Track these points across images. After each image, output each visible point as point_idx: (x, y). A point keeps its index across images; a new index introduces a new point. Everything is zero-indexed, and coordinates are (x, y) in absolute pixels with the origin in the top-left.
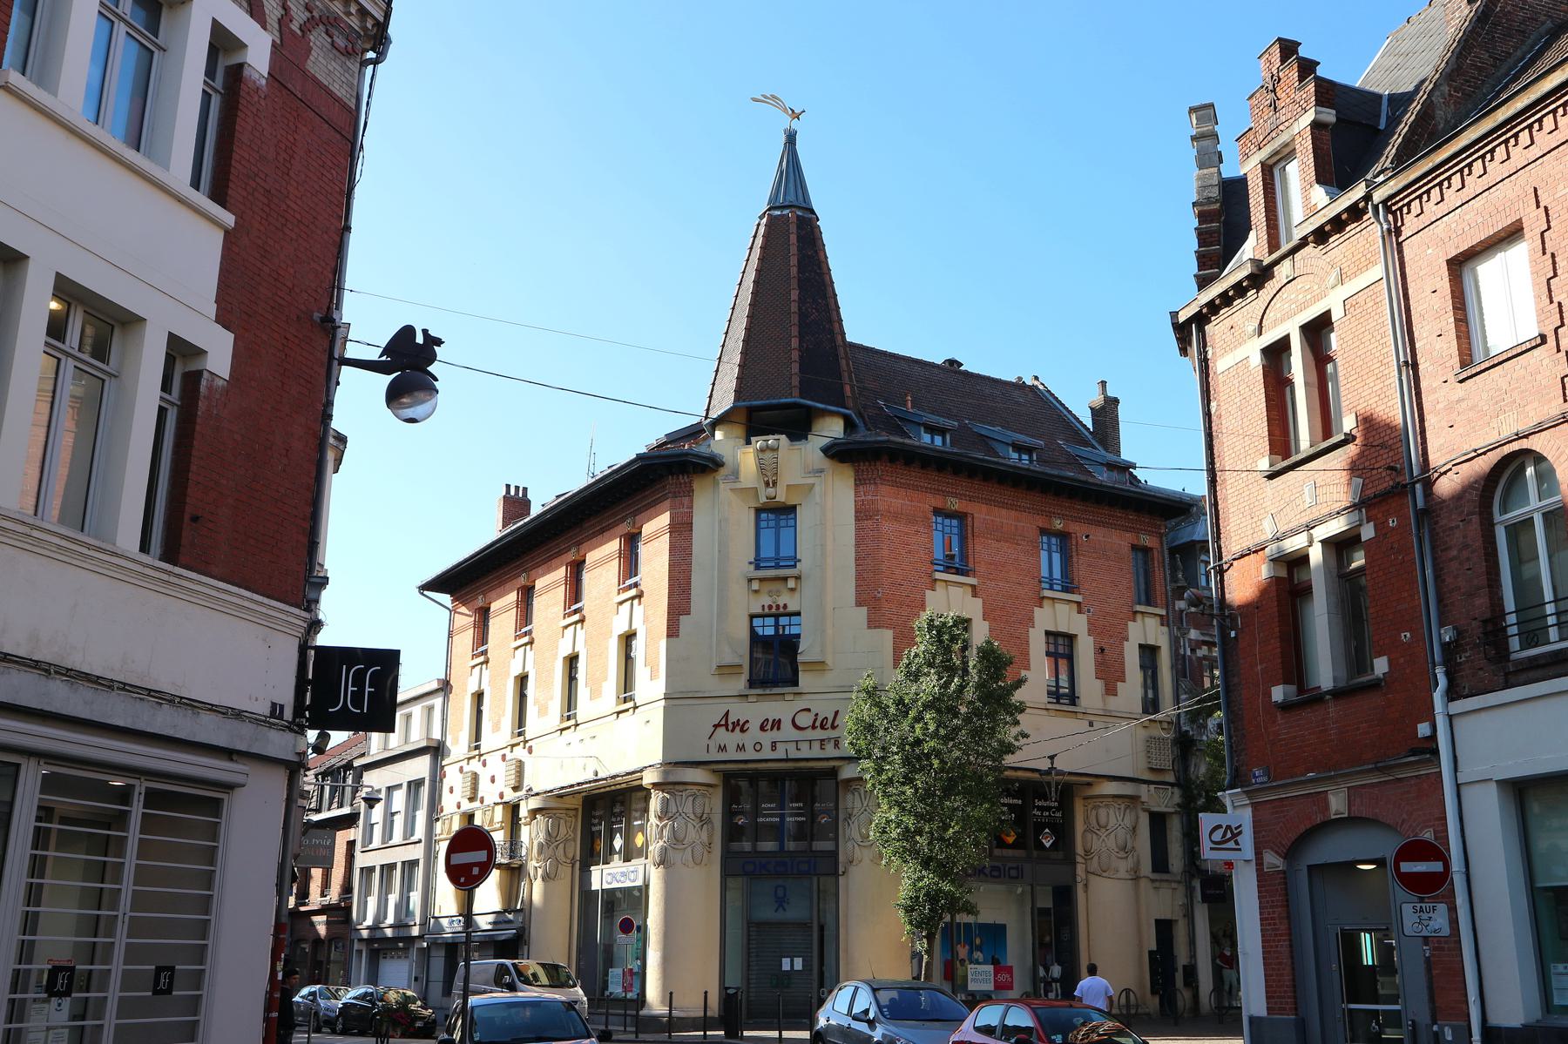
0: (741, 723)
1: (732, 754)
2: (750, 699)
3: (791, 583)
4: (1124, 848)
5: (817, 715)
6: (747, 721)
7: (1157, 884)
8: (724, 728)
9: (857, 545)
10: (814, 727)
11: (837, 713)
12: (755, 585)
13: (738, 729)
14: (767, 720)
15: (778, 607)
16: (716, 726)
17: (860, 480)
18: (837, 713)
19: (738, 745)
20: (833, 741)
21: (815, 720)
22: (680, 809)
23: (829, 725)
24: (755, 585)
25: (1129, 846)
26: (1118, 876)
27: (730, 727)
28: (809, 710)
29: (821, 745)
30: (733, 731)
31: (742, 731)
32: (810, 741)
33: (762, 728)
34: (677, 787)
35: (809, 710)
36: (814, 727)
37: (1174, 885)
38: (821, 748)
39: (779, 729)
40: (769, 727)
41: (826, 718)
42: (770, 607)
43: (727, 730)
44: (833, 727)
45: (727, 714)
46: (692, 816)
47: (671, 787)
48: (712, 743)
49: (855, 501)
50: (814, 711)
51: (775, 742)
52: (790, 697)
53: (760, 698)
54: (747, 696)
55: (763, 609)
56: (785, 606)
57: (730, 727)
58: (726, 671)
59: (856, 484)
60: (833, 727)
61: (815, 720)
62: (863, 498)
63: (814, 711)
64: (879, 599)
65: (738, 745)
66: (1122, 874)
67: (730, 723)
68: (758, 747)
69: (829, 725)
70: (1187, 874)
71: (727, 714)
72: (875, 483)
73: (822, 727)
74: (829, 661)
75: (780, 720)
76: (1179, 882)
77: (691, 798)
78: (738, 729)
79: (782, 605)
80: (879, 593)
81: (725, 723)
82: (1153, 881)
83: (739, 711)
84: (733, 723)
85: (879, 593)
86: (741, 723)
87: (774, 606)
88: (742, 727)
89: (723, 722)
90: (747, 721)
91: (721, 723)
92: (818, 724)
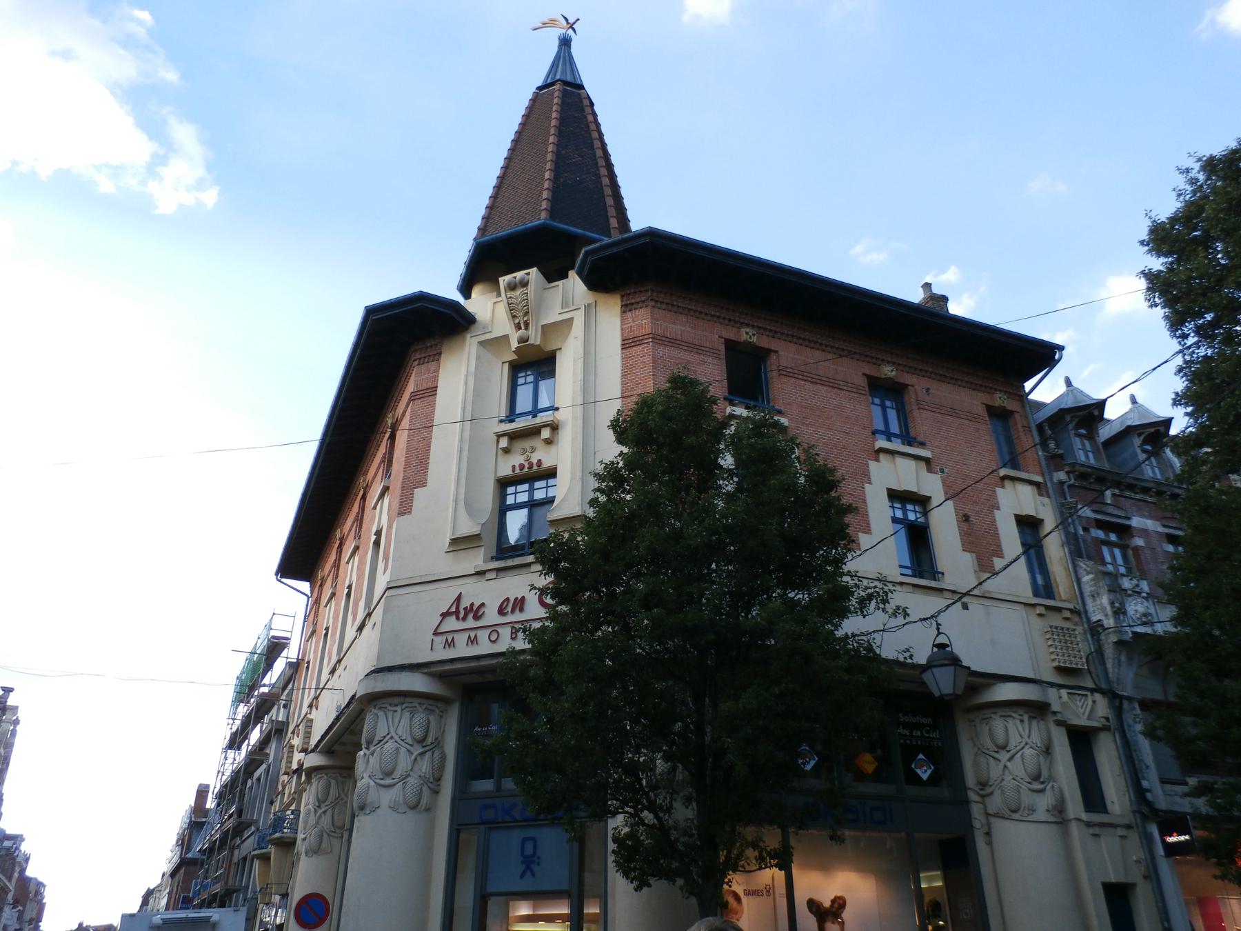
0: (475, 609)
1: (463, 649)
3: (546, 433)
4: (1037, 778)
7: (1097, 830)
8: (453, 618)
12: (504, 443)
13: (471, 616)
14: (508, 599)
16: (445, 615)
22: (392, 730)
25: (1045, 773)
26: (1035, 817)
27: (462, 615)
30: (464, 619)
31: (476, 618)
33: (501, 611)
37: (1120, 832)
39: (521, 610)
40: (509, 609)
42: (522, 467)
43: (458, 618)
55: (514, 471)
57: (462, 615)
66: (1041, 815)
68: (494, 637)
70: (1137, 815)
76: (1129, 827)
78: (471, 616)
79: (535, 462)
81: (456, 610)
82: (1089, 824)
83: (475, 592)
84: (465, 609)
86: (475, 609)
88: (476, 612)
89: (453, 609)
90: (483, 605)
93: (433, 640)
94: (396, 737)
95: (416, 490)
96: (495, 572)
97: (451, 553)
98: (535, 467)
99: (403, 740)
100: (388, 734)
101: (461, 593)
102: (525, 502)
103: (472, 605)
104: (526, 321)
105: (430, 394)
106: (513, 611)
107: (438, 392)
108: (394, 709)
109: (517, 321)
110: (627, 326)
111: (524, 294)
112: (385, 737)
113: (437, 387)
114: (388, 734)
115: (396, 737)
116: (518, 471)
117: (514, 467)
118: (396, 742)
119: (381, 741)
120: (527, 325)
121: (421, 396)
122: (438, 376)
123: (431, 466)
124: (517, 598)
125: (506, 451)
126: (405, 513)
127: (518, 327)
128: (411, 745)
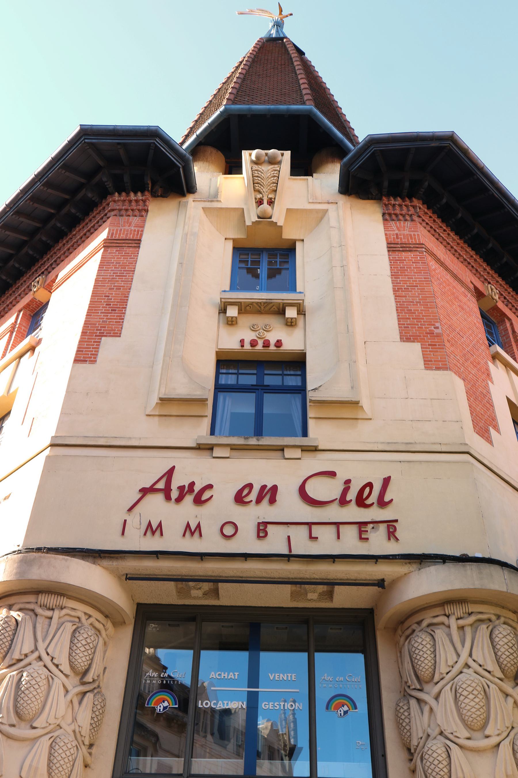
0: (197, 488)
2: (217, 452)
5: (348, 482)
6: (210, 487)
8: (160, 497)
9: (394, 275)
10: (343, 501)
11: (387, 481)
12: (232, 312)
14: (250, 486)
15: (267, 344)
16: (145, 492)
17: (390, 214)
18: (387, 481)
19: (188, 525)
20: (383, 528)
21: (346, 491)
22: (41, 646)
23: (373, 498)
24: (232, 312)
27: (175, 494)
28: (332, 474)
29: (361, 532)
30: (179, 500)
31: (198, 501)
32: (337, 524)
34: (43, 599)
35: (332, 474)
36: (343, 501)
38: (361, 538)
39: (272, 501)
40: (253, 496)
41: (370, 485)
42: (253, 343)
43: (168, 498)
44: (382, 503)
45: (170, 473)
46: (66, 667)
47: (31, 598)
48: (133, 520)
49: (386, 234)
50: (342, 476)
51: (266, 524)
52: (297, 453)
53: (235, 453)
54: (210, 448)
55: (242, 346)
56: (279, 344)
57: (175, 494)
58: (174, 410)
59: (385, 220)
60: (382, 503)
61: (346, 491)
62: (397, 232)
63: (342, 476)
64: (439, 336)
65: (188, 525)
67: (174, 486)
69: (373, 498)
71: (170, 473)
72: (412, 220)
73: (361, 502)
74: (365, 403)
75: (274, 489)
77: (69, 628)
78: (189, 499)
79: (273, 342)
80: (437, 328)
84: (181, 488)
85: (437, 328)
86: (197, 488)
87: (260, 343)
89: (161, 485)
90: (210, 487)
91: (158, 486)
92: (352, 495)
93: (125, 521)
94: (47, 659)
95: (103, 338)
96: (229, 449)
97: (156, 419)
98: (272, 347)
99: (57, 666)
100: (32, 652)
101: (174, 467)
102: (252, 385)
103: (192, 484)
104: (271, 199)
105: (130, 245)
106: (259, 500)
107: (141, 246)
108: (49, 613)
109: (259, 196)
110: (391, 232)
111: (275, 170)
112: (26, 656)
113: (140, 240)
114: (32, 652)
115: (47, 659)
116: (247, 346)
117: (242, 341)
118: (45, 666)
119: (20, 660)
120: (271, 202)
121: (117, 245)
122: (142, 231)
123: (127, 317)
124: (264, 487)
125: (231, 322)
126: (86, 361)
127: (260, 202)
128: (67, 676)
